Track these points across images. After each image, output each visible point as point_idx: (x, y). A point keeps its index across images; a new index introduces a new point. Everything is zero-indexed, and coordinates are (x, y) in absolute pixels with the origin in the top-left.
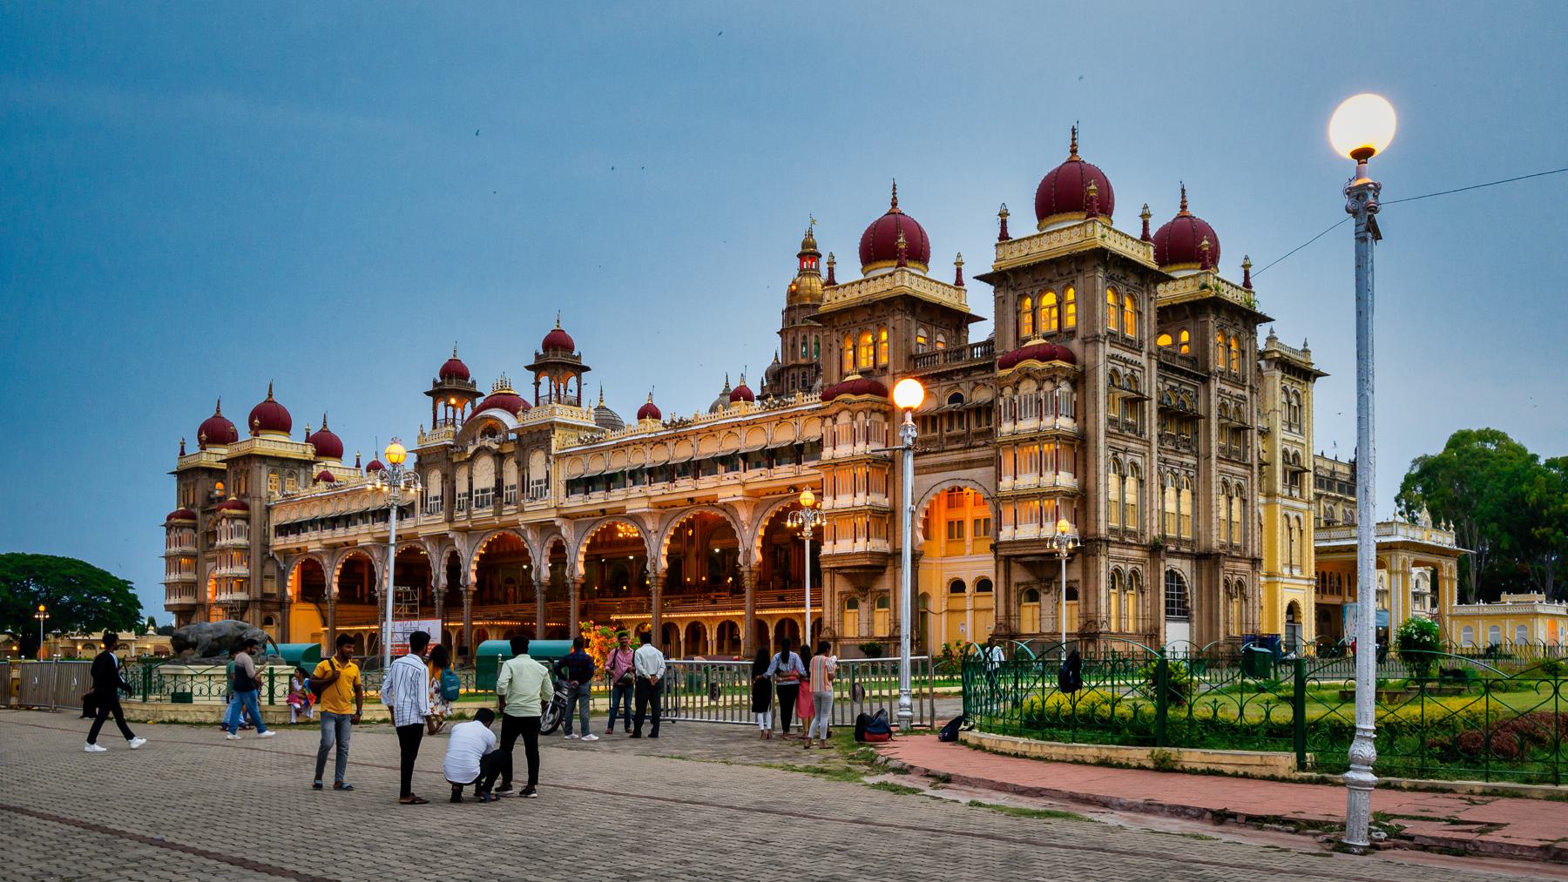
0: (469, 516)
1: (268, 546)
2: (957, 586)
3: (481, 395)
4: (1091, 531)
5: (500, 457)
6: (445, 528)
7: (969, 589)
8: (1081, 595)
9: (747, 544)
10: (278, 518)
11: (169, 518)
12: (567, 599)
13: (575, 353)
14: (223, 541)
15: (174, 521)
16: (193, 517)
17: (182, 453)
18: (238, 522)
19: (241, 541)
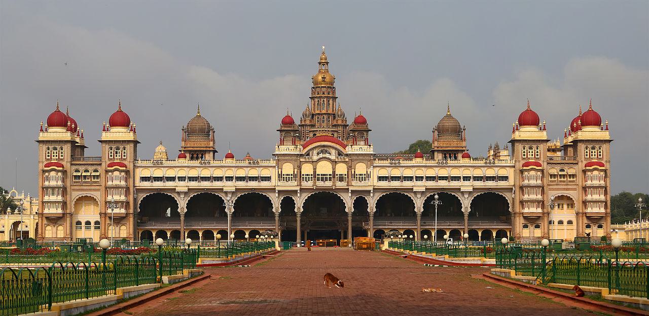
0: (315, 183)
5: (334, 163)
10: (147, 173)
16: (63, 167)
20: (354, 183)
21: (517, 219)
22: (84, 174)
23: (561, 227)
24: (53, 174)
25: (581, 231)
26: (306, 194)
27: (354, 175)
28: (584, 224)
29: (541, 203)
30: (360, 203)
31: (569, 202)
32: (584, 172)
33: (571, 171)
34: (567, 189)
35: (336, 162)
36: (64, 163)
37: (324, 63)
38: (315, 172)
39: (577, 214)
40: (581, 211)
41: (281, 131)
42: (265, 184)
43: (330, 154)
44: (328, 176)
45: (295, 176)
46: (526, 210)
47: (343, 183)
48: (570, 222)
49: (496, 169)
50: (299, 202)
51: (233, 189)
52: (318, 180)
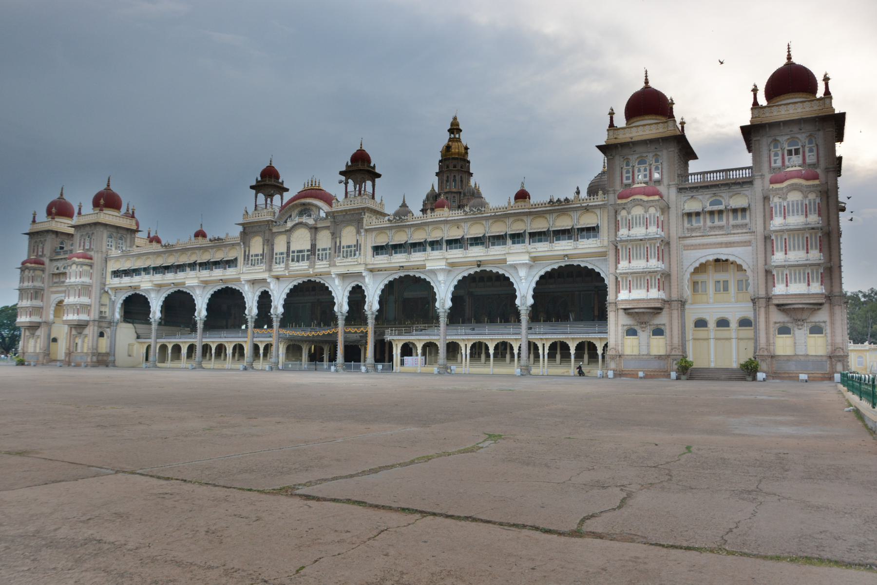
0: (287, 267)
1: (105, 285)
2: (701, 323)
3: (287, 190)
4: (836, 290)
5: (314, 229)
6: (265, 275)
7: (712, 325)
8: (829, 331)
9: (523, 292)
11: (23, 263)
12: (366, 324)
13: (280, 181)
14: (72, 280)
15: (29, 265)
17: (34, 221)
18: (85, 268)
19: (86, 280)
20: (338, 261)
23: (723, 332)
24: (27, 272)
26: (285, 285)
28: (771, 325)
29: (664, 278)
31: (739, 275)
32: (766, 199)
33: (737, 202)
35: (316, 228)
37: (455, 129)
38: (288, 248)
39: (754, 301)
41: (252, 187)
42: (230, 273)
44: (306, 253)
46: (624, 295)
47: (324, 262)
48: (745, 323)
49: (575, 215)
52: (293, 260)
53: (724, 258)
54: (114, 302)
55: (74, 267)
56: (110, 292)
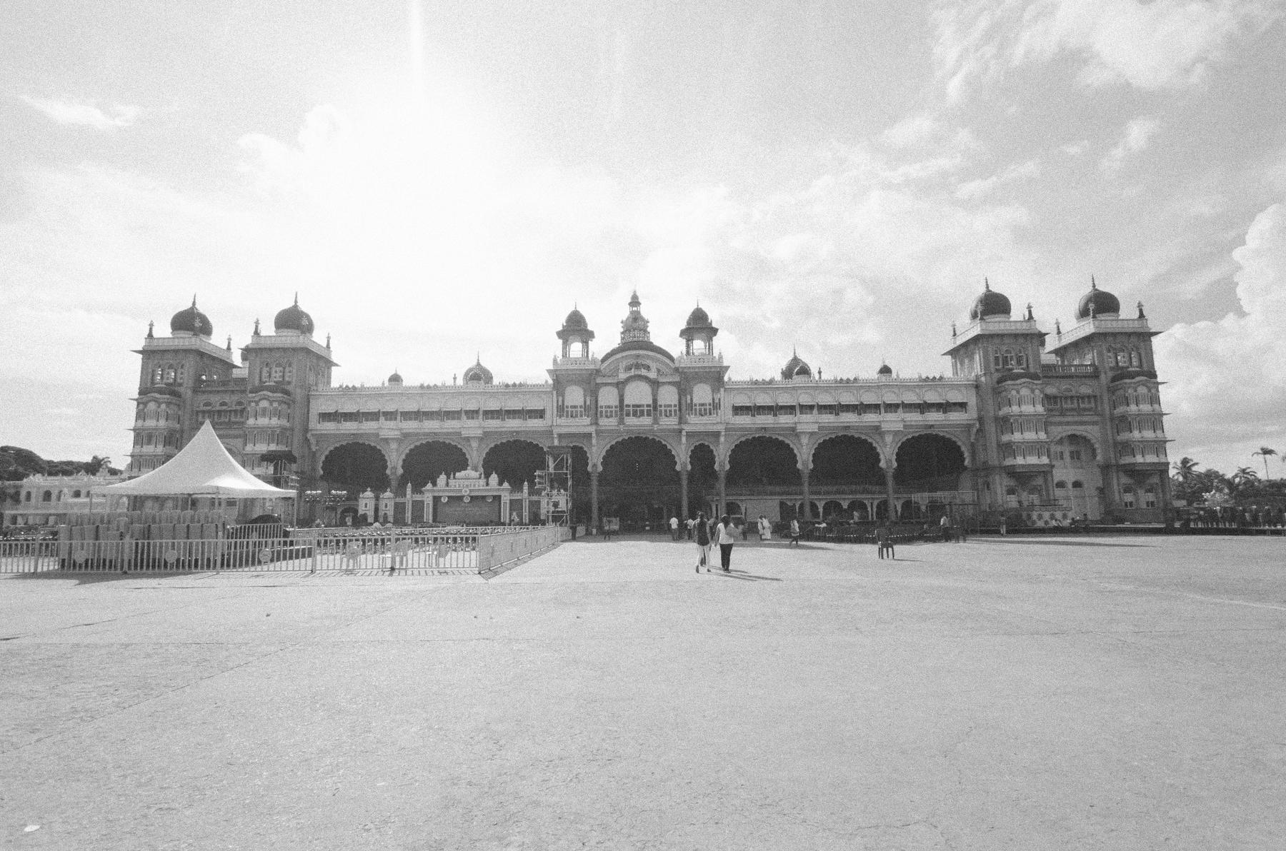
0: (621, 421)
1: (306, 430)
5: (655, 384)
20: (693, 419)
21: (997, 477)
22: (218, 408)
25: (1117, 497)
27: (691, 406)
30: (702, 455)
33: (1085, 390)
34: (1082, 423)
36: (182, 390)
37: (635, 302)
38: (621, 400)
39: (1105, 468)
40: (1113, 462)
42: (534, 424)
43: (648, 368)
45: (586, 408)
48: (1077, 484)
50: (596, 456)
51: (479, 432)
52: (628, 415)
53: (1078, 433)
54: (314, 453)
55: (264, 404)
56: (313, 441)
